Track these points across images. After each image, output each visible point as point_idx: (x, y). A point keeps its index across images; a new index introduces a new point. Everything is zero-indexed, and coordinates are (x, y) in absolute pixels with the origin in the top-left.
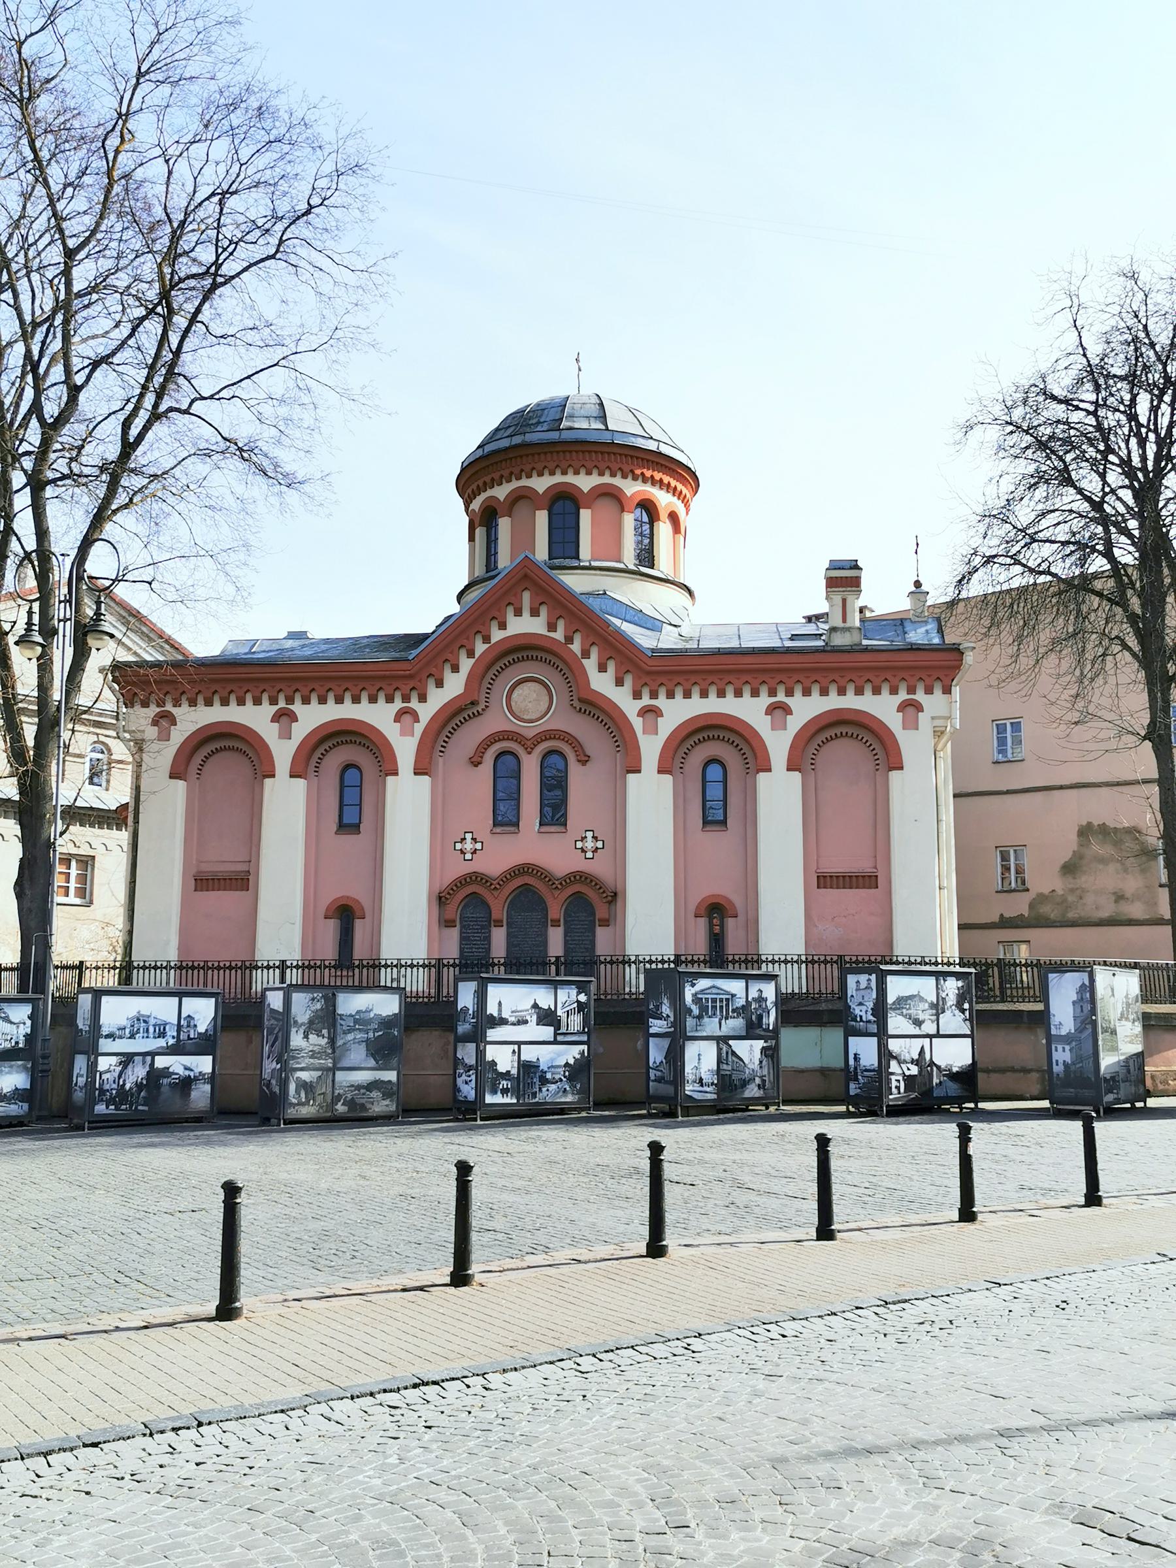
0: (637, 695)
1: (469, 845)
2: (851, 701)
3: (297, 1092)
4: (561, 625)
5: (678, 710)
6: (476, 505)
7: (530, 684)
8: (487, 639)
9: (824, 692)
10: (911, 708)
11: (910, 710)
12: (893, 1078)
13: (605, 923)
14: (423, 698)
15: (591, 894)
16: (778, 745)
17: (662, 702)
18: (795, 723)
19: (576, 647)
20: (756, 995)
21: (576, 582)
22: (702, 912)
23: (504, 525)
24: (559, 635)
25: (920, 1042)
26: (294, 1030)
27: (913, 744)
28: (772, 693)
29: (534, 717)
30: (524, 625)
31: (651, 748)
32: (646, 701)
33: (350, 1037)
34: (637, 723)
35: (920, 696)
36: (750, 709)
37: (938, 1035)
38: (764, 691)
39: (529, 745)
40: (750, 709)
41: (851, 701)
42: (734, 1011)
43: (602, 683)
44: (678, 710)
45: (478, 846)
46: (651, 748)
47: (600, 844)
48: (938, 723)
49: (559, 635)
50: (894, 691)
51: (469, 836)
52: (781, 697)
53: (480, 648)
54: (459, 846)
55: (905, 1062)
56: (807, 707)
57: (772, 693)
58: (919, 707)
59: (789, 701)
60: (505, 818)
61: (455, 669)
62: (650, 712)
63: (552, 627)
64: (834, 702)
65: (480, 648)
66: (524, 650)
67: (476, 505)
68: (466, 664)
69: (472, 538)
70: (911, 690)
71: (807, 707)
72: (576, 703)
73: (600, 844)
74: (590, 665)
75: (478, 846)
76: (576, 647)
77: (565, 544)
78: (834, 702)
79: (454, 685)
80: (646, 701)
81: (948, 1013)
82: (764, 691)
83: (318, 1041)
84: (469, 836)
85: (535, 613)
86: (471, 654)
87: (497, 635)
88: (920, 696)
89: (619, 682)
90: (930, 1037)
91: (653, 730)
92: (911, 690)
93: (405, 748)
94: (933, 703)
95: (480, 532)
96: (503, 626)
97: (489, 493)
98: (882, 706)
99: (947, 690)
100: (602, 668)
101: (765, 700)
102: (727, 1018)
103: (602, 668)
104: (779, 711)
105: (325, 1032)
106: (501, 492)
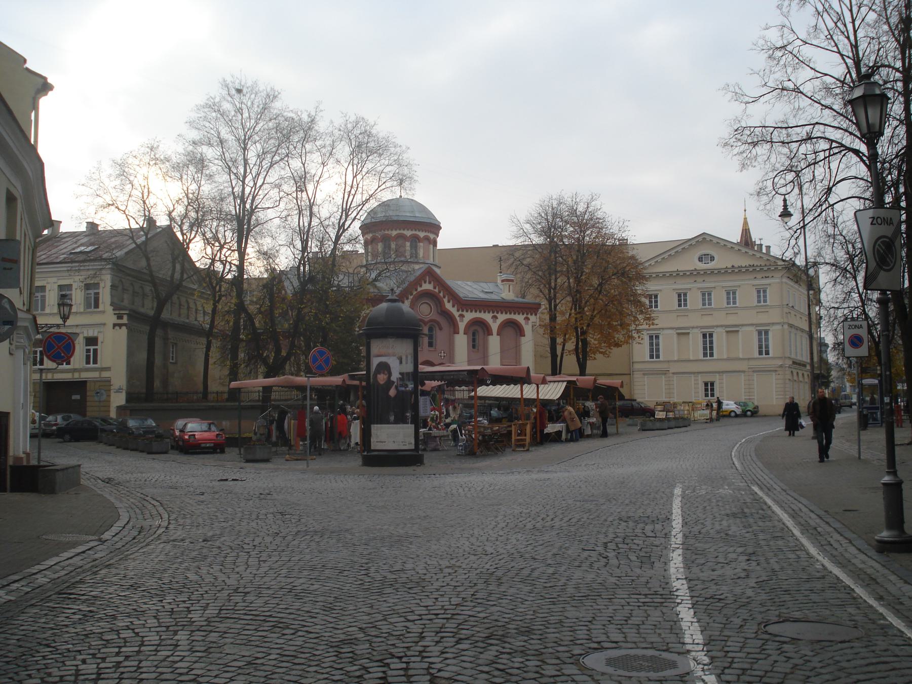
0: (458, 311)
5: (469, 316)
10: (527, 319)
16: (495, 327)
17: (464, 313)
18: (499, 321)
19: (441, 294)
24: (437, 290)
27: (528, 329)
30: (427, 286)
31: (462, 326)
34: (458, 319)
35: (529, 316)
36: (487, 317)
39: (425, 323)
40: (487, 317)
43: (448, 306)
44: (469, 316)
46: (462, 326)
49: (437, 290)
53: (415, 293)
56: (502, 317)
63: (435, 288)
65: (415, 293)
66: (427, 294)
71: (502, 317)
74: (446, 300)
76: (441, 294)
85: (430, 283)
87: (419, 289)
88: (529, 316)
89: (453, 306)
91: (462, 321)
94: (533, 318)
96: (421, 286)
98: (520, 318)
100: (449, 302)
101: (491, 314)
103: (449, 302)
104: (495, 318)
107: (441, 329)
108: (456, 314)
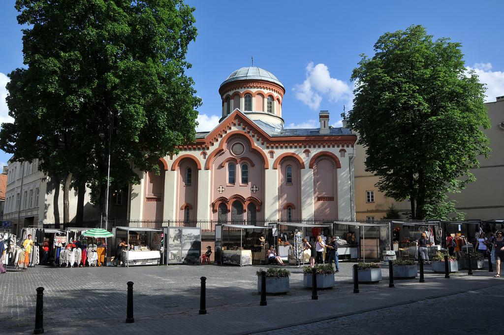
1: (221, 189)
2: (326, 149)
3: (171, 256)
4: (246, 128)
6: (224, 97)
7: (239, 145)
8: (226, 132)
9: (319, 147)
10: (343, 151)
11: (343, 152)
13: (259, 211)
14: (208, 149)
15: (254, 202)
17: (275, 150)
21: (252, 118)
22: (286, 208)
23: (232, 102)
26: (170, 239)
27: (344, 161)
28: (305, 147)
29: (239, 154)
33: (186, 241)
34: (268, 156)
35: (345, 148)
38: (303, 147)
41: (326, 149)
43: (256, 145)
44: (279, 152)
45: (224, 189)
46: (271, 162)
47: (257, 189)
48: (350, 155)
50: (338, 147)
51: (221, 187)
52: (307, 148)
53: (224, 135)
54: (218, 189)
56: (314, 152)
57: (305, 147)
58: (345, 151)
59: (310, 149)
60: (232, 181)
61: (217, 140)
62: (272, 153)
63: (244, 129)
64: (321, 150)
67: (224, 97)
68: (220, 139)
69: (223, 105)
70: (343, 146)
71: (314, 152)
72: (251, 150)
73: (257, 189)
75: (224, 189)
77: (249, 106)
78: (321, 150)
79: (216, 145)
82: (303, 147)
83: (177, 242)
84: (221, 187)
86: (221, 136)
87: (228, 131)
88: (345, 148)
91: (272, 157)
92: (343, 146)
93: (202, 161)
94: (349, 150)
95: (226, 104)
96: (230, 128)
97: (228, 93)
98: (335, 151)
99: (353, 146)
101: (303, 150)
105: (179, 240)
106: (231, 93)
107: (253, 165)
108: (266, 152)
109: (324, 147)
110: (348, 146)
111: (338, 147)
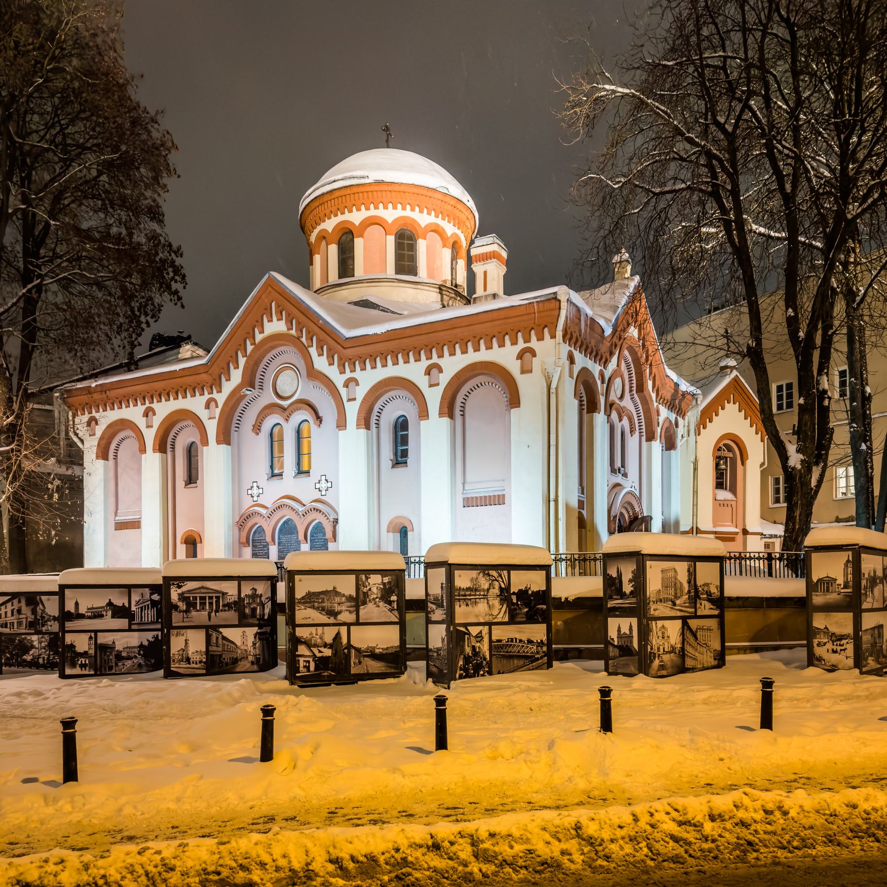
0: (343, 372)
12: (301, 660)
17: (358, 374)
20: (250, 593)
25: (335, 630)
28: (429, 358)
32: (348, 374)
35: (534, 344)
37: (358, 623)
40: (413, 370)
41: (484, 355)
42: (224, 606)
44: (369, 377)
50: (514, 342)
52: (435, 359)
55: (316, 646)
56: (453, 364)
64: (473, 357)
70: (527, 340)
71: (453, 364)
78: (473, 357)
80: (348, 374)
81: (370, 606)
88: (534, 344)
90: (349, 625)
92: (527, 340)
98: (505, 355)
102: (217, 611)
109: (477, 349)
110: (540, 338)
111: (514, 342)
